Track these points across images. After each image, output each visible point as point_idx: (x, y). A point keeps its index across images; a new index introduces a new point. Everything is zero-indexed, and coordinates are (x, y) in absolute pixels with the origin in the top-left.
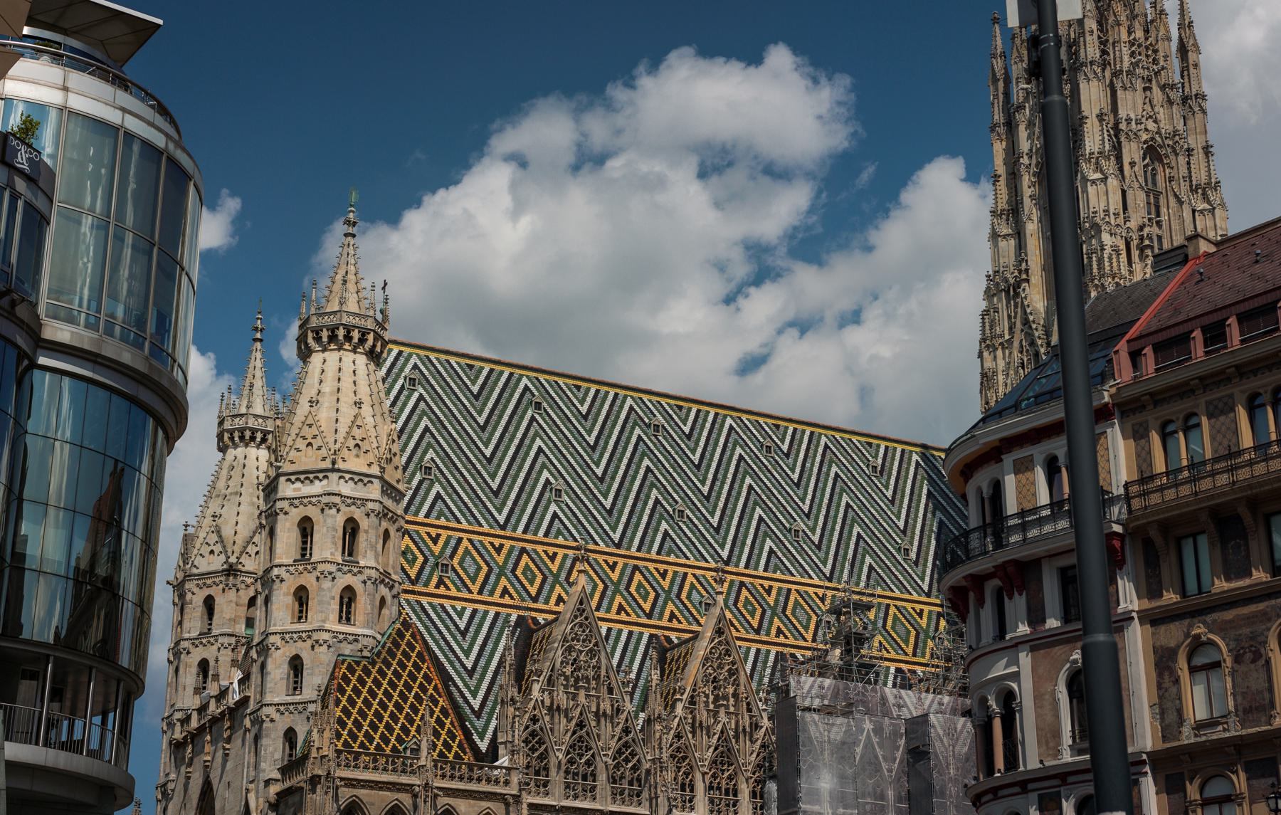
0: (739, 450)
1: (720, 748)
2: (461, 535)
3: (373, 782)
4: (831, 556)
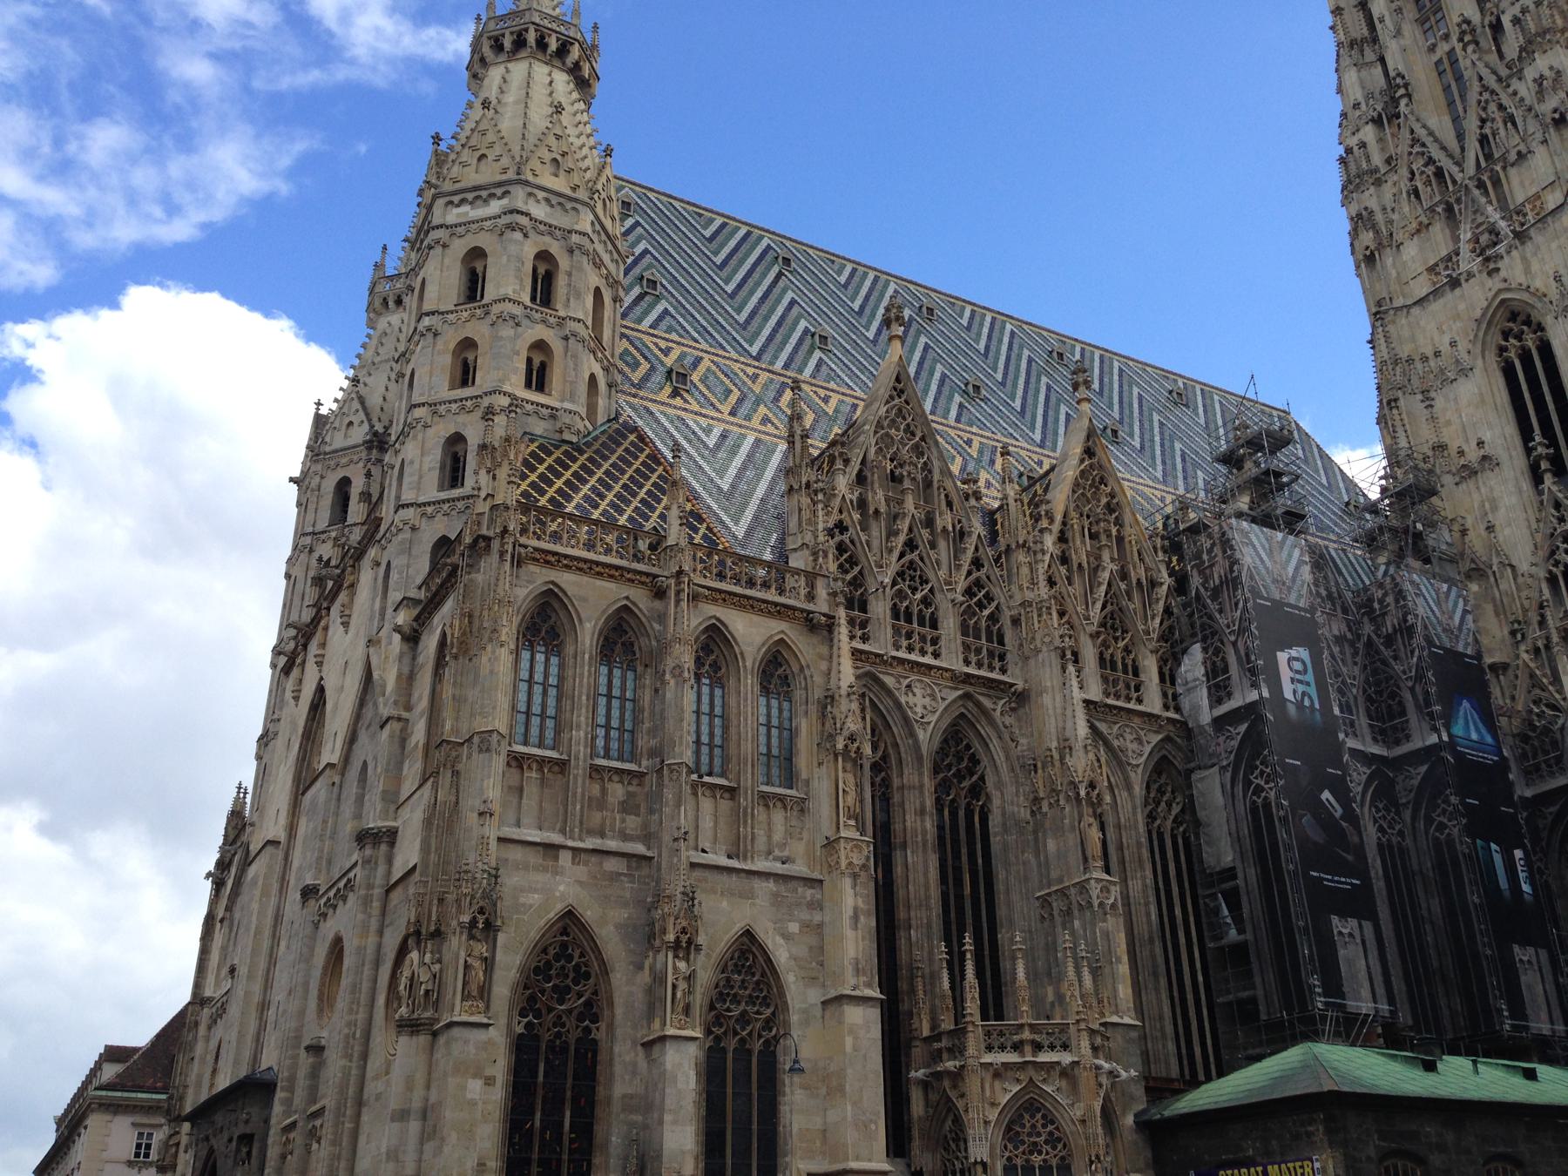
0: (1026, 353)
1: (1109, 608)
2: (701, 354)
3: (585, 561)
4: (1159, 461)
